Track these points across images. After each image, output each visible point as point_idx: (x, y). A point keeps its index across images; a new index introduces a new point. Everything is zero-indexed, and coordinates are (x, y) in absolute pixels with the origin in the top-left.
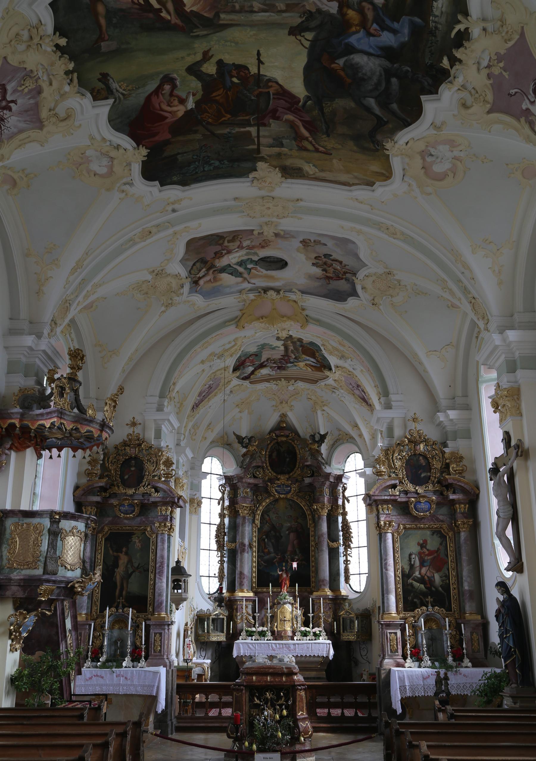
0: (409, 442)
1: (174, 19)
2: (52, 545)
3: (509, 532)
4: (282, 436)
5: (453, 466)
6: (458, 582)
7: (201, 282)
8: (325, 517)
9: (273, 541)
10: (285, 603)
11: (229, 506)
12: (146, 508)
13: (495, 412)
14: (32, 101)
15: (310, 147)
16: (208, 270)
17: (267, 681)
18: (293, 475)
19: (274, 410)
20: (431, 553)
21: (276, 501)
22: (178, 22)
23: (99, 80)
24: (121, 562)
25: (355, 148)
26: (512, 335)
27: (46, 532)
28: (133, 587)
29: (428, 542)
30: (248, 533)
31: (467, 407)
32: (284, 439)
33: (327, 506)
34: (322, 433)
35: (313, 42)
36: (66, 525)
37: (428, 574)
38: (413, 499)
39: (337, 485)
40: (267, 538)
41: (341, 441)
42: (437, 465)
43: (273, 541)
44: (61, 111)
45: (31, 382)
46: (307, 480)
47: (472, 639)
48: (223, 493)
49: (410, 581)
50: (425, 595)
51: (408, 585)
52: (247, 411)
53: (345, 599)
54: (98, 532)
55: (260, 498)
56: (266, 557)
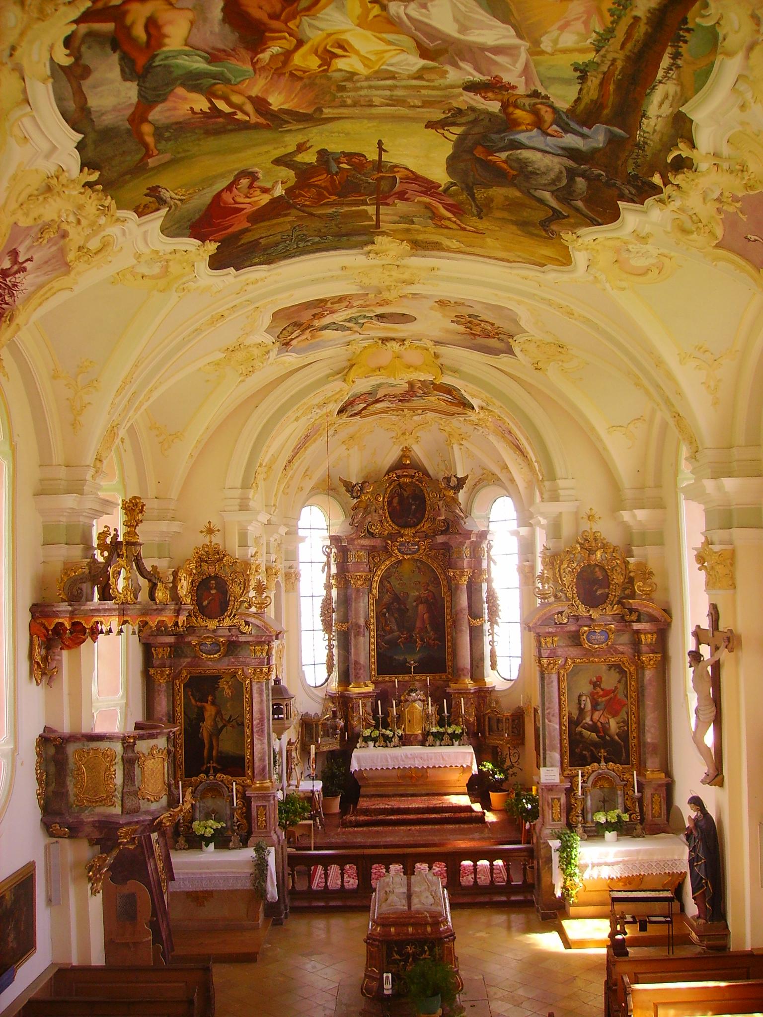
0: (582, 548)
1: (254, 118)
2: (129, 777)
3: (709, 738)
5: (638, 584)
6: (639, 730)
7: (294, 343)
10: (415, 701)
11: (337, 574)
12: (232, 647)
13: (700, 569)
14: (54, 248)
15: (454, 226)
16: (303, 331)
17: (407, 934)
20: (606, 693)
21: (400, 562)
22: (261, 120)
23: (146, 195)
24: (207, 715)
25: (519, 232)
26: (729, 484)
27: (118, 759)
28: (226, 745)
29: (603, 679)
30: (365, 608)
31: (659, 504)
33: (468, 571)
34: (460, 475)
35: (462, 138)
36: (142, 746)
37: (602, 720)
38: (586, 628)
39: (481, 542)
41: (485, 482)
42: (618, 578)
44: (94, 244)
45: (76, 552)
46: (440, 539)
47: (652, 802)
48: (328, 556)
49: (579, 729)
50: (596, 745)
51: (576, 734)
53: (491, 691)
54: (174, 679)
55: (377, 559)
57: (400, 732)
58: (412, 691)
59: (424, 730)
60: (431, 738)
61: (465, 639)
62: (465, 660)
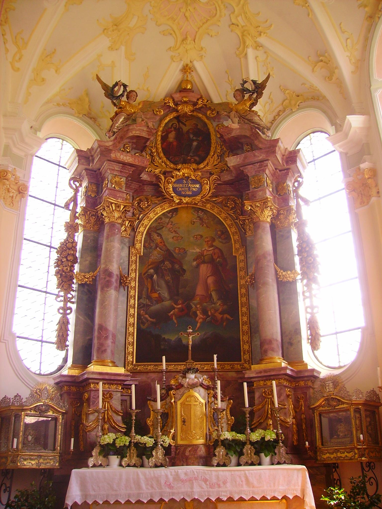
4: (185, 102)
8: (268, 225)
9: (168, 278)
10: (193, 386)
11: (85, 210)
18: (204, 167)
19: (172, 58)
21: (175, 211)
32: (187, 109)
40: (156, 272)
41: (287, 111)
43: (168, 278)
52: (123, 48)
55: (144, 205)
56: (155, 307)
57: (168, 441)
58: (189, 369)
59: (208, 437)
60: (221, 451)
61: (271, 296)
62: (273, 328)
